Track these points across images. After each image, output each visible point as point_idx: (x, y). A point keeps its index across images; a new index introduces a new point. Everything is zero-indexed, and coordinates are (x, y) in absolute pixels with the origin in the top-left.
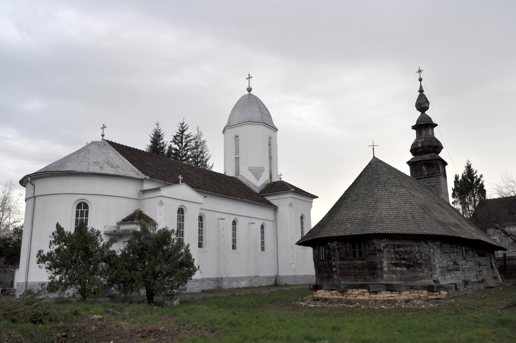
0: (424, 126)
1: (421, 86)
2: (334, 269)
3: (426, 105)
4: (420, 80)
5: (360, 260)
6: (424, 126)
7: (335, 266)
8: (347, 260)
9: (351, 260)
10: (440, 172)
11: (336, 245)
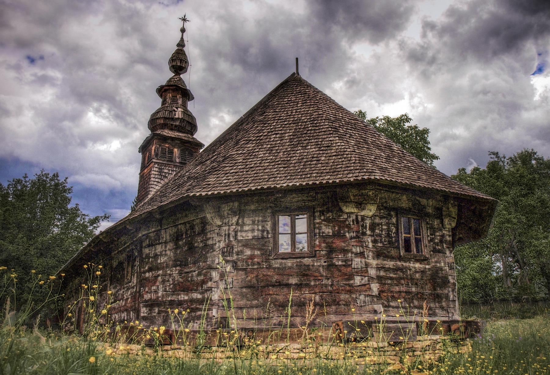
1: (182, 39)
2: (357, 280)
5: (417, 261)
7: (363, 272)
8: (392, 258)
9: (400, 258)
11: (371, 214)
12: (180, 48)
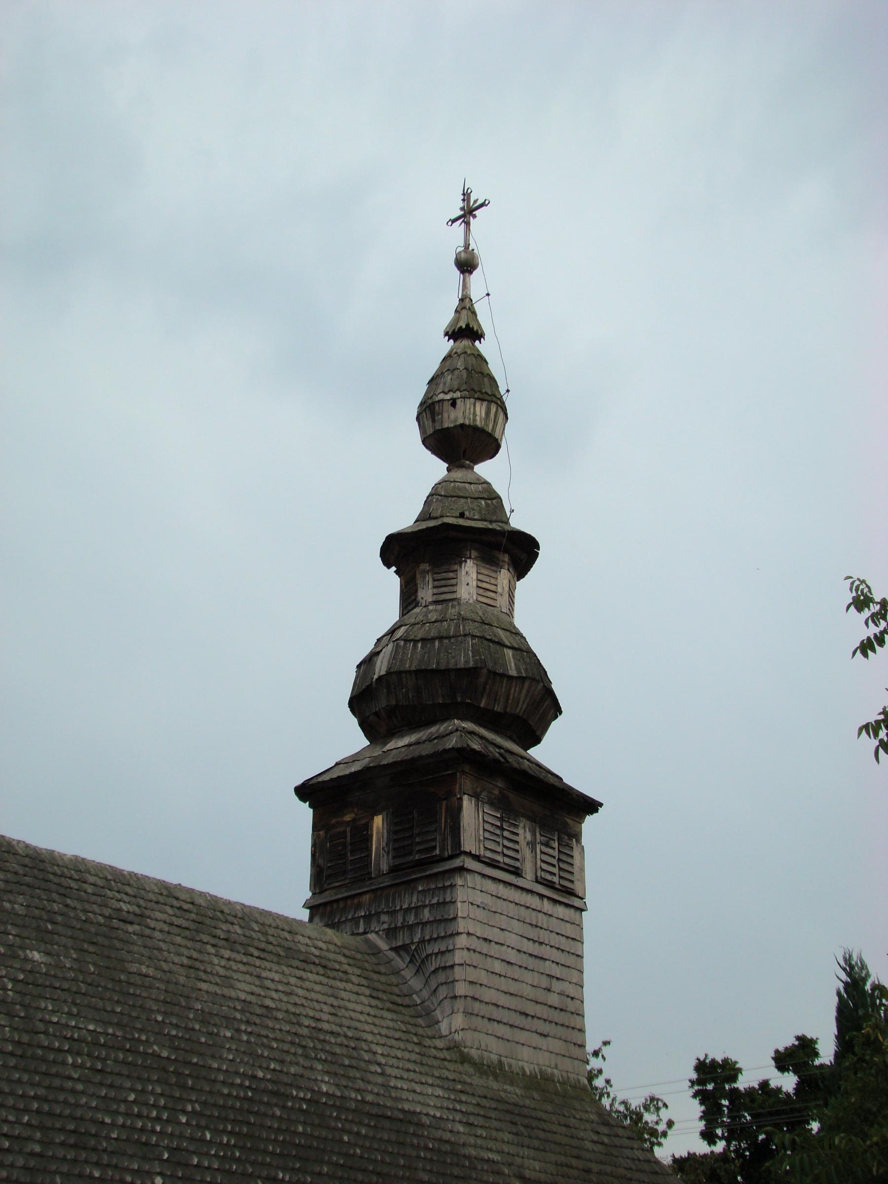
0: (457, 544)
3: (473, 412)
4: (466, 265)
6: (457, 544)
10: (459, 852)
12: (466, 343)
